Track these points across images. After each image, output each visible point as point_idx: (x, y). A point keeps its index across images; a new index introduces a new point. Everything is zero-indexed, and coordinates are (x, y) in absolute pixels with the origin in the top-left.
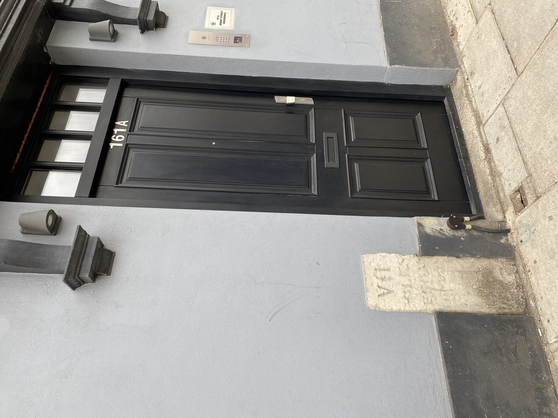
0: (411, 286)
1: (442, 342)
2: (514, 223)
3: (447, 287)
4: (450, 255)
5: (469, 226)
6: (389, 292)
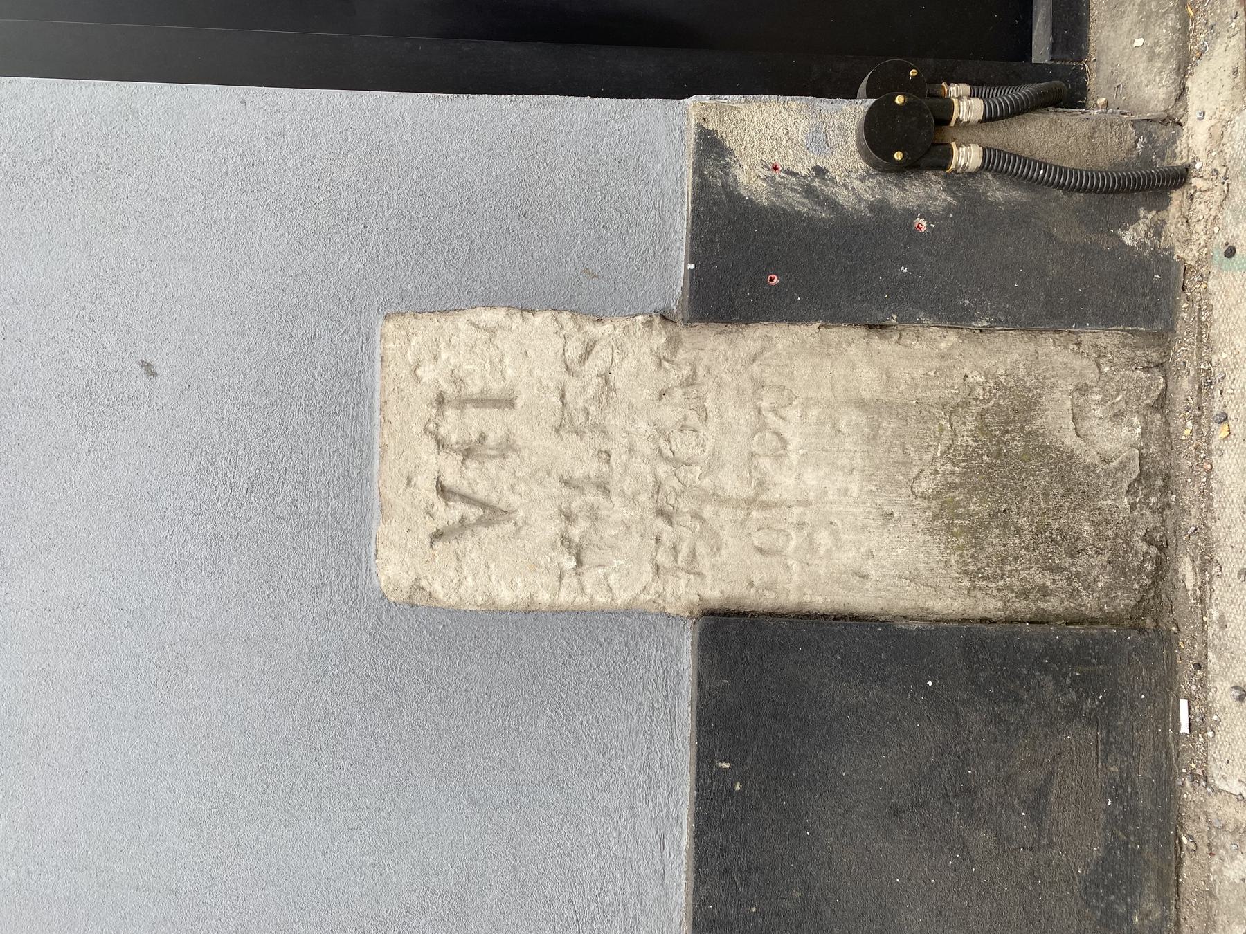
0: (603, 487)
1: (703, 761)
2: (1217, 139)
3: (784, 485)
4: (833, 316)
5: (967, 156)
6: (492, 514)
